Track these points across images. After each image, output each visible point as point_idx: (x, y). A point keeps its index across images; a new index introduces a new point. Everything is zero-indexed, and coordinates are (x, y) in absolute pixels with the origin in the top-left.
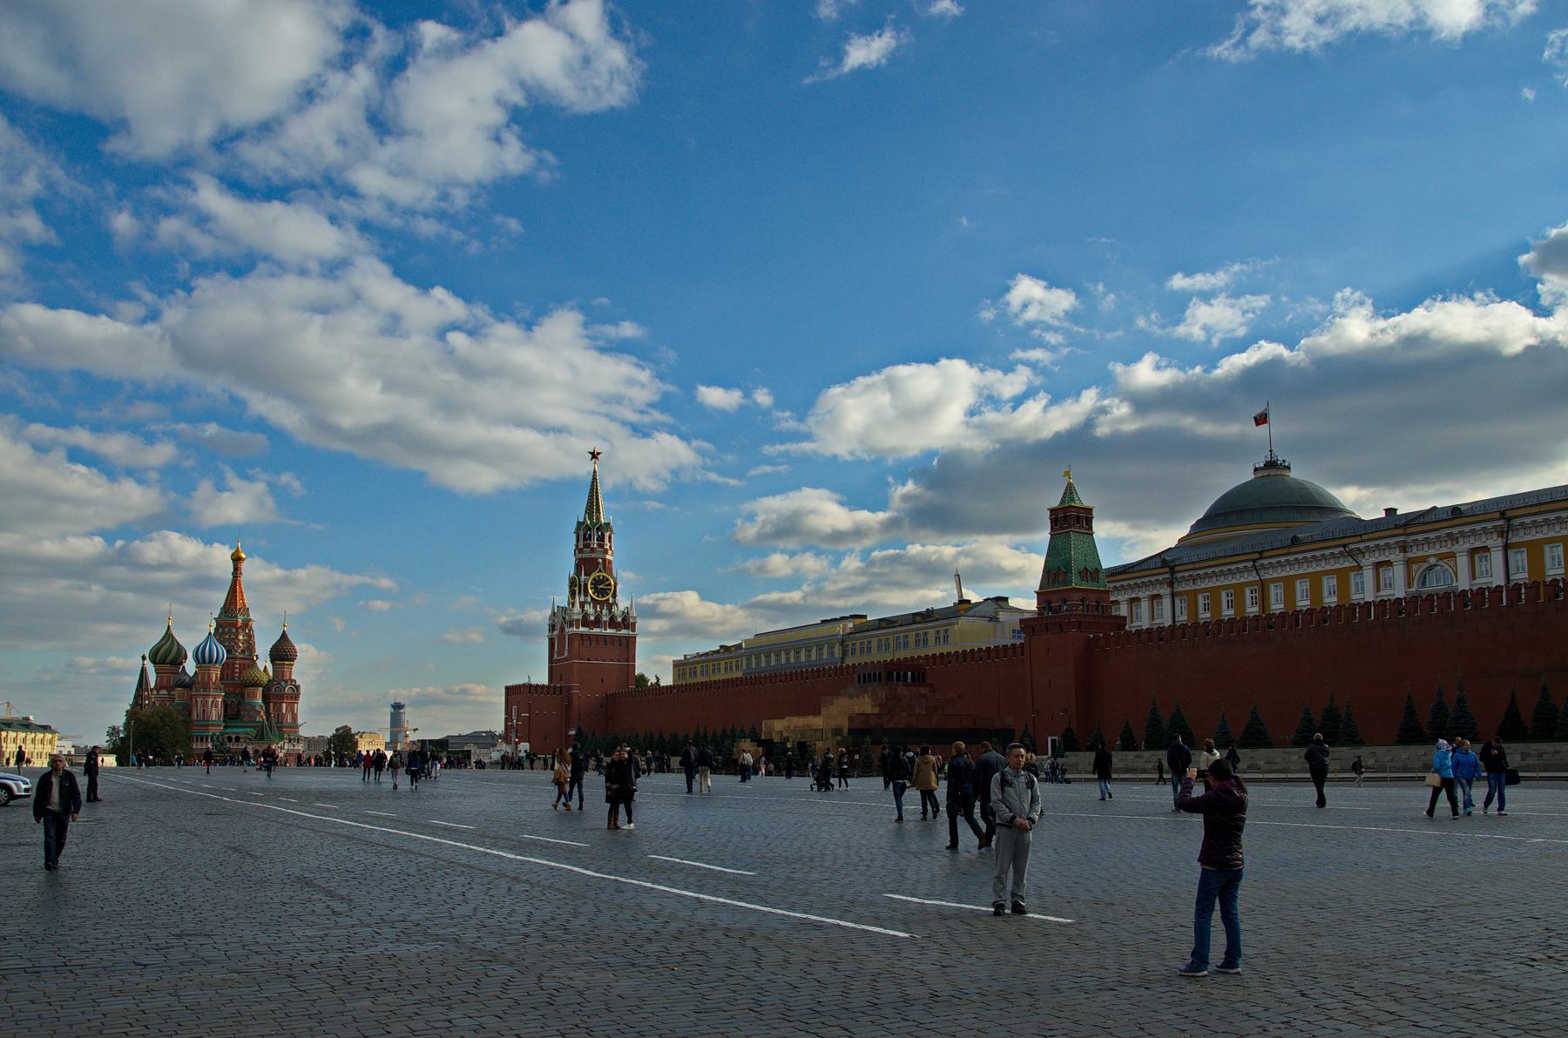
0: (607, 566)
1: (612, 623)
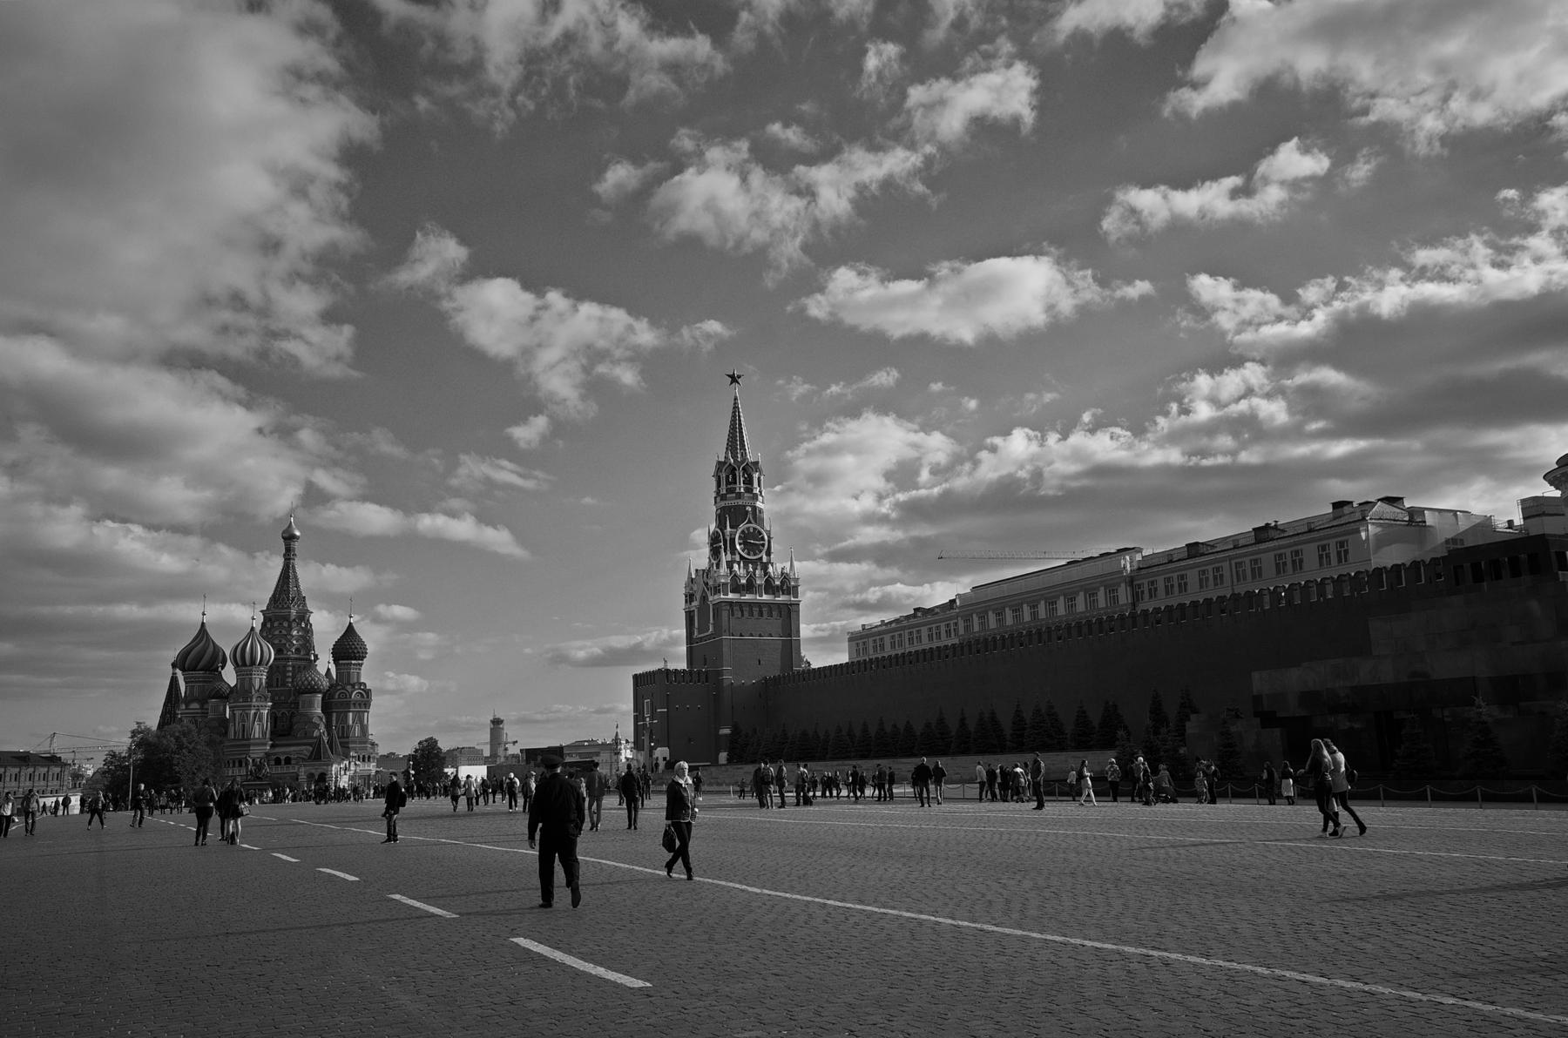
0: (757, 515)
1: (769, 587)
